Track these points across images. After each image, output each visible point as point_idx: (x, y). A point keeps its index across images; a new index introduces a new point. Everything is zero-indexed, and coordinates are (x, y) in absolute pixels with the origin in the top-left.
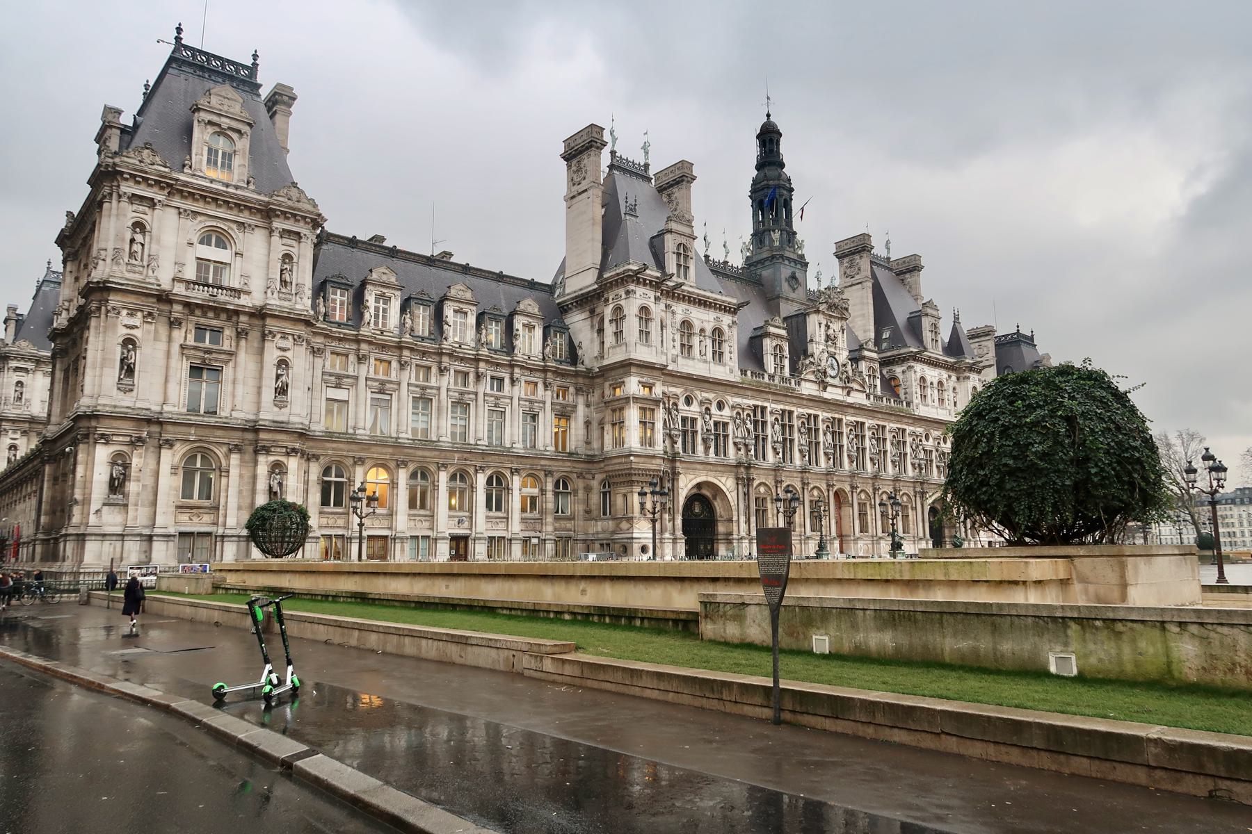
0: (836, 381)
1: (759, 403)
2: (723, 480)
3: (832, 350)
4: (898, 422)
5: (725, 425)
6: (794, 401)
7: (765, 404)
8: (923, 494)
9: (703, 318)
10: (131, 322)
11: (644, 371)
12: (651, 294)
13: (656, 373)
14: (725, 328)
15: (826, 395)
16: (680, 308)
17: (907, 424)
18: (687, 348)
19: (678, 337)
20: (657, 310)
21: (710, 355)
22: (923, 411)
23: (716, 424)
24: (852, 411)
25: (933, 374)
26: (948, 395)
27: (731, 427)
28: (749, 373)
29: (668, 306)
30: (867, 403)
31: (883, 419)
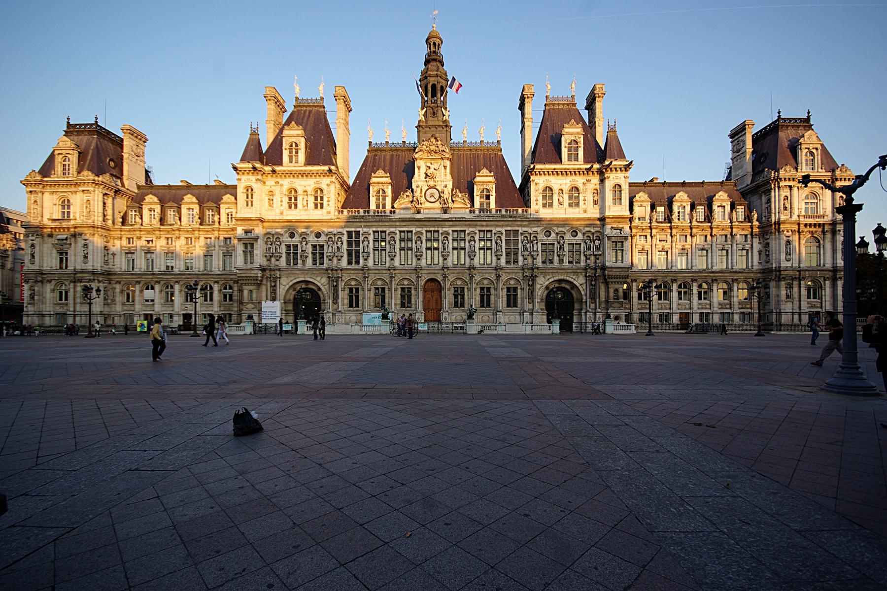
0: (437, 205)
1: (353, 230)
2: (318, 279)
3: (432, 183)
4: (510, 226)
5: (322, 246)
6: (387, 224)
7: (358, 229)
8: (532, 280)
9: (309, 184)
10: (33, 238)
11: (247, 223)
12: (253, 178)
13: (255, 222)
14: (324, 187)
15: (418, 216)
16: (286, 183)
17: (518, 226)
18: (293, 203)
19: (286, 199)
20: (256, 186)
21: (311, 205)
22: (546, 213)
23: (314, 246)
24: (451, 223)
25: (556, 183)
26: (587, 197)
27: (326, 247)
28: (345, 211)
29: (277, 183)
30: (471, 216)
31: (487, 226)
